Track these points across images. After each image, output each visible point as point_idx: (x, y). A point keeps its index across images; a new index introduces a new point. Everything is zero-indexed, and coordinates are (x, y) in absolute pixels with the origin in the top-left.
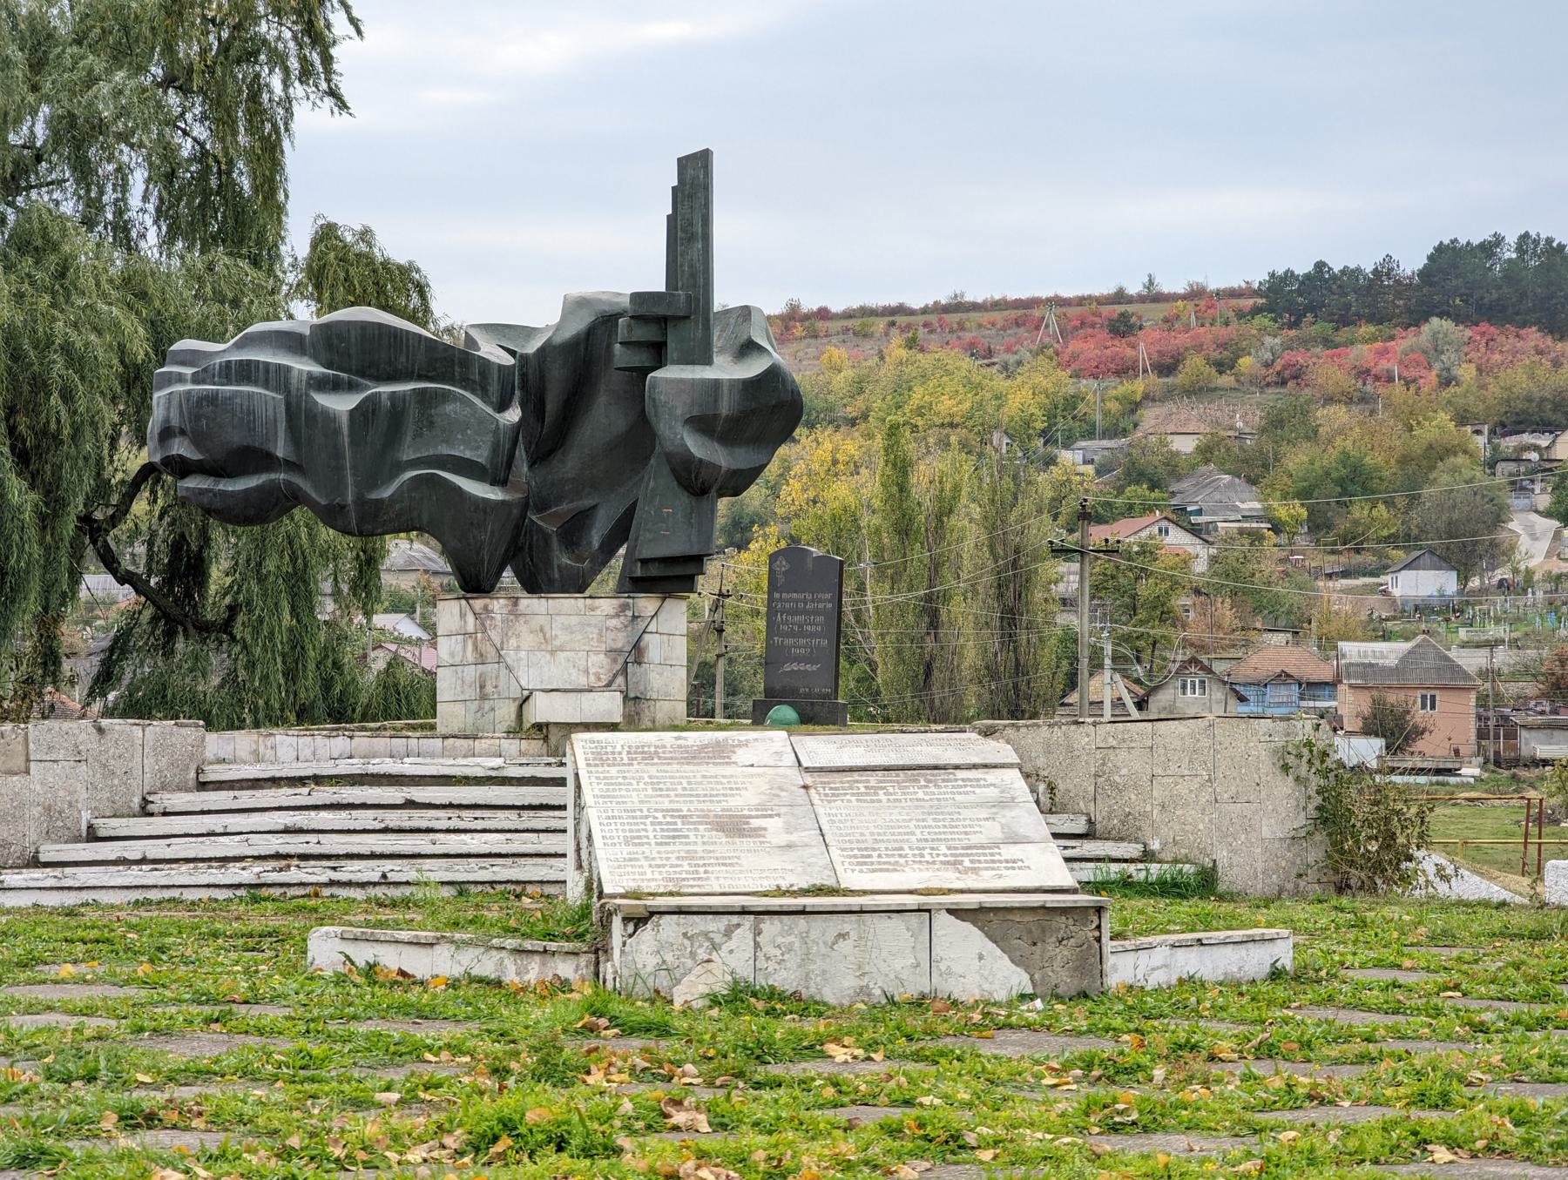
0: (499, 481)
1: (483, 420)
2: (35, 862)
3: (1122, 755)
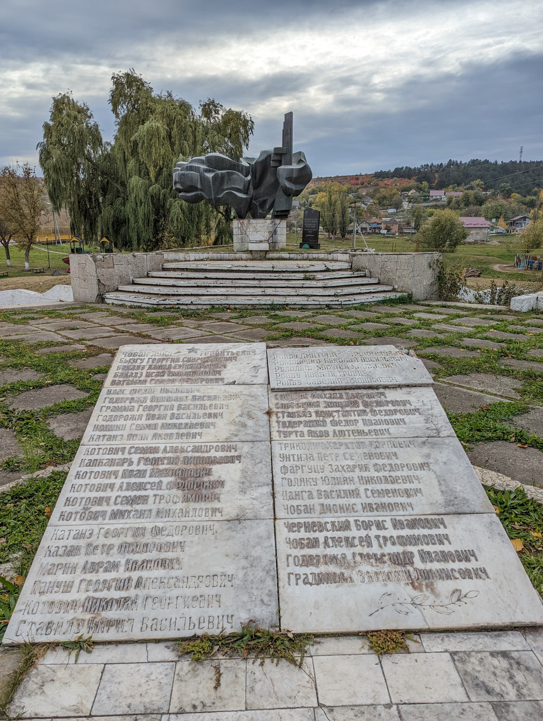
0: (246, 193)
1: (242, 178)
2: (117, 290)
3: (389, 263)
